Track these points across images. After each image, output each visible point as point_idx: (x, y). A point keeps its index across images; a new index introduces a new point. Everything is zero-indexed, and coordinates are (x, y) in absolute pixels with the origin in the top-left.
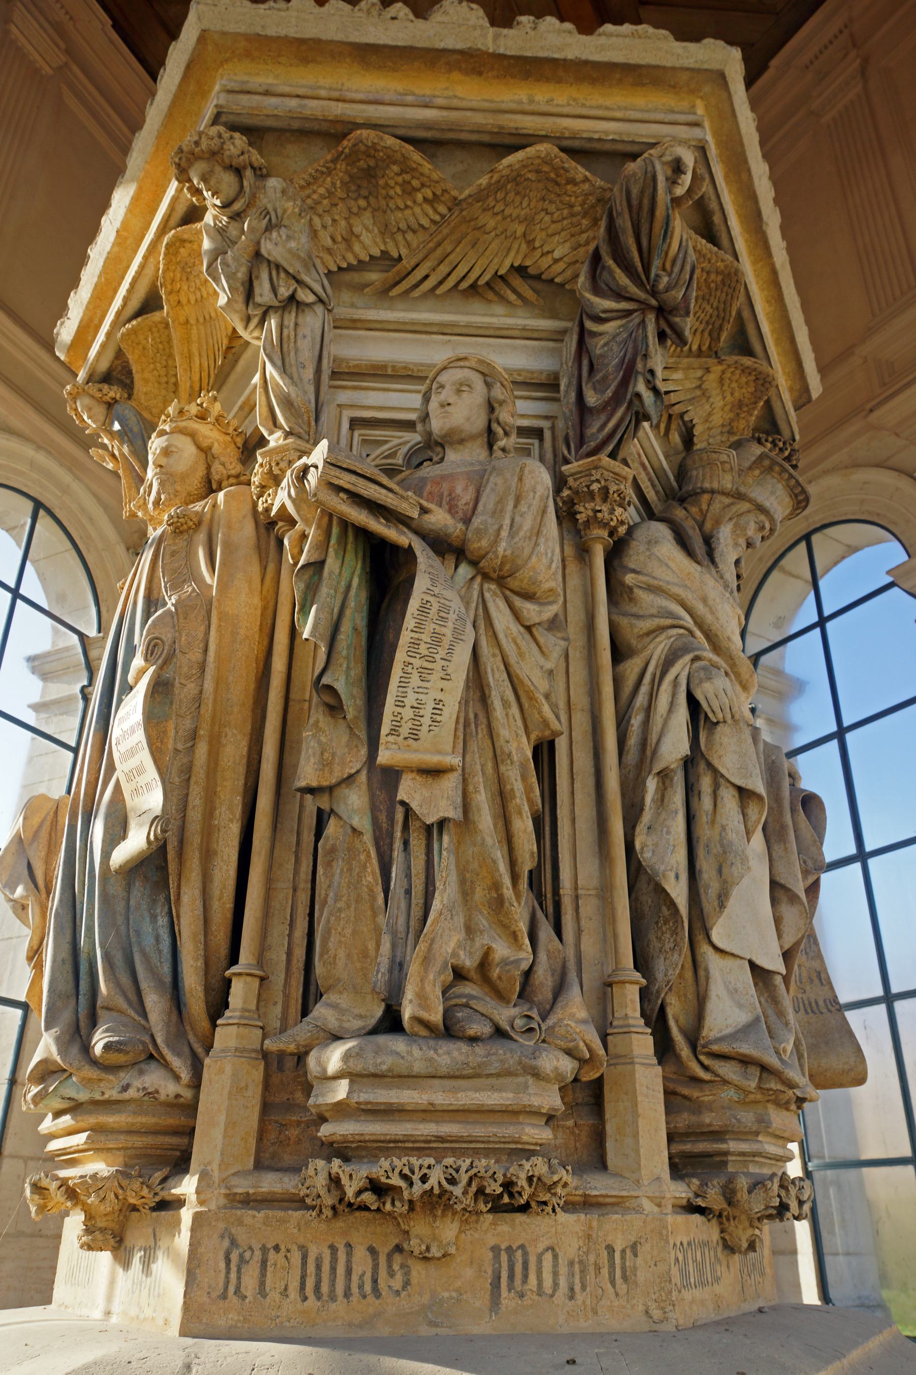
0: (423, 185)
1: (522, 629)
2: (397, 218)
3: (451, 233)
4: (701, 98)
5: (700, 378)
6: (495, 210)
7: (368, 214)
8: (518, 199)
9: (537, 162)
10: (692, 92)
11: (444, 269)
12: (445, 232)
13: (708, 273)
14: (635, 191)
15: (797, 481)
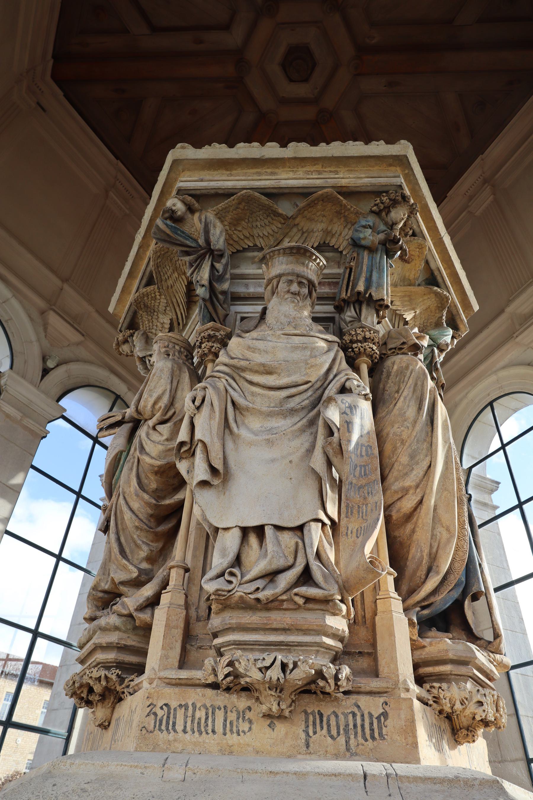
0: (154, 293)
1: (151, 432)
2: (162, 308)
3: (170, 296)
4: (183, 171)
5: (299, 230)
6: (167, 278)
7: (159, 314)
8: (165, 269)
9: (154, 256)
10: (179, 175)
11: (181, 306)
12: (168, 298)
13: (238, 208)
14: (158, 236)
15: (283, 249)
